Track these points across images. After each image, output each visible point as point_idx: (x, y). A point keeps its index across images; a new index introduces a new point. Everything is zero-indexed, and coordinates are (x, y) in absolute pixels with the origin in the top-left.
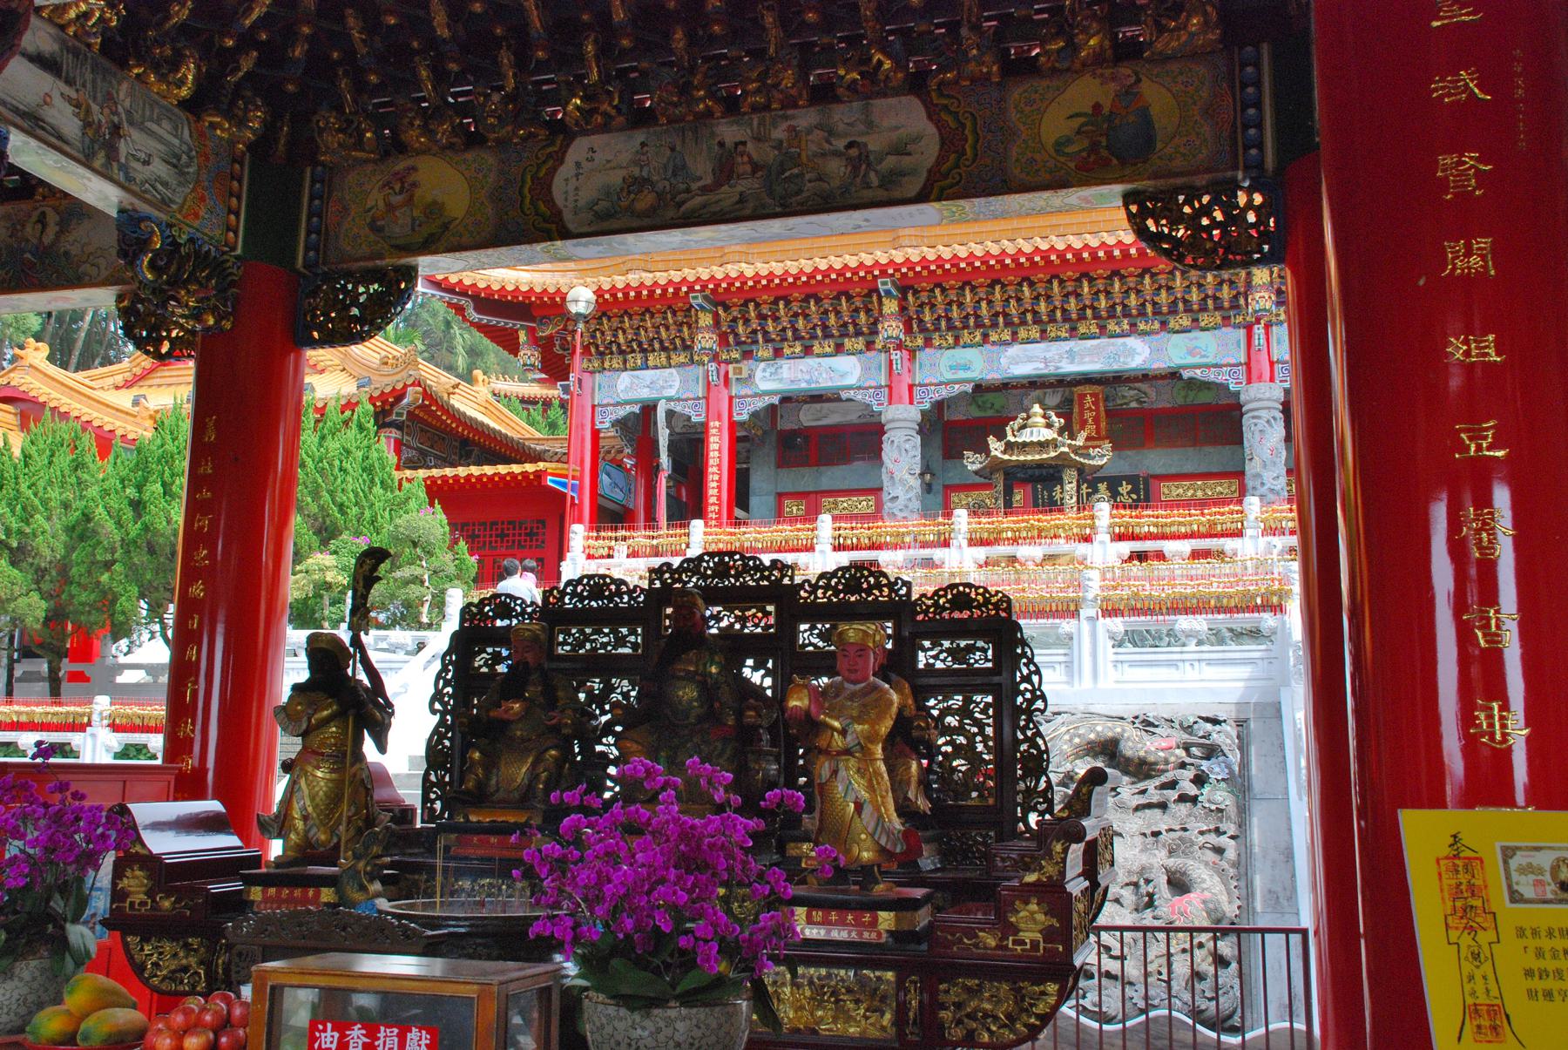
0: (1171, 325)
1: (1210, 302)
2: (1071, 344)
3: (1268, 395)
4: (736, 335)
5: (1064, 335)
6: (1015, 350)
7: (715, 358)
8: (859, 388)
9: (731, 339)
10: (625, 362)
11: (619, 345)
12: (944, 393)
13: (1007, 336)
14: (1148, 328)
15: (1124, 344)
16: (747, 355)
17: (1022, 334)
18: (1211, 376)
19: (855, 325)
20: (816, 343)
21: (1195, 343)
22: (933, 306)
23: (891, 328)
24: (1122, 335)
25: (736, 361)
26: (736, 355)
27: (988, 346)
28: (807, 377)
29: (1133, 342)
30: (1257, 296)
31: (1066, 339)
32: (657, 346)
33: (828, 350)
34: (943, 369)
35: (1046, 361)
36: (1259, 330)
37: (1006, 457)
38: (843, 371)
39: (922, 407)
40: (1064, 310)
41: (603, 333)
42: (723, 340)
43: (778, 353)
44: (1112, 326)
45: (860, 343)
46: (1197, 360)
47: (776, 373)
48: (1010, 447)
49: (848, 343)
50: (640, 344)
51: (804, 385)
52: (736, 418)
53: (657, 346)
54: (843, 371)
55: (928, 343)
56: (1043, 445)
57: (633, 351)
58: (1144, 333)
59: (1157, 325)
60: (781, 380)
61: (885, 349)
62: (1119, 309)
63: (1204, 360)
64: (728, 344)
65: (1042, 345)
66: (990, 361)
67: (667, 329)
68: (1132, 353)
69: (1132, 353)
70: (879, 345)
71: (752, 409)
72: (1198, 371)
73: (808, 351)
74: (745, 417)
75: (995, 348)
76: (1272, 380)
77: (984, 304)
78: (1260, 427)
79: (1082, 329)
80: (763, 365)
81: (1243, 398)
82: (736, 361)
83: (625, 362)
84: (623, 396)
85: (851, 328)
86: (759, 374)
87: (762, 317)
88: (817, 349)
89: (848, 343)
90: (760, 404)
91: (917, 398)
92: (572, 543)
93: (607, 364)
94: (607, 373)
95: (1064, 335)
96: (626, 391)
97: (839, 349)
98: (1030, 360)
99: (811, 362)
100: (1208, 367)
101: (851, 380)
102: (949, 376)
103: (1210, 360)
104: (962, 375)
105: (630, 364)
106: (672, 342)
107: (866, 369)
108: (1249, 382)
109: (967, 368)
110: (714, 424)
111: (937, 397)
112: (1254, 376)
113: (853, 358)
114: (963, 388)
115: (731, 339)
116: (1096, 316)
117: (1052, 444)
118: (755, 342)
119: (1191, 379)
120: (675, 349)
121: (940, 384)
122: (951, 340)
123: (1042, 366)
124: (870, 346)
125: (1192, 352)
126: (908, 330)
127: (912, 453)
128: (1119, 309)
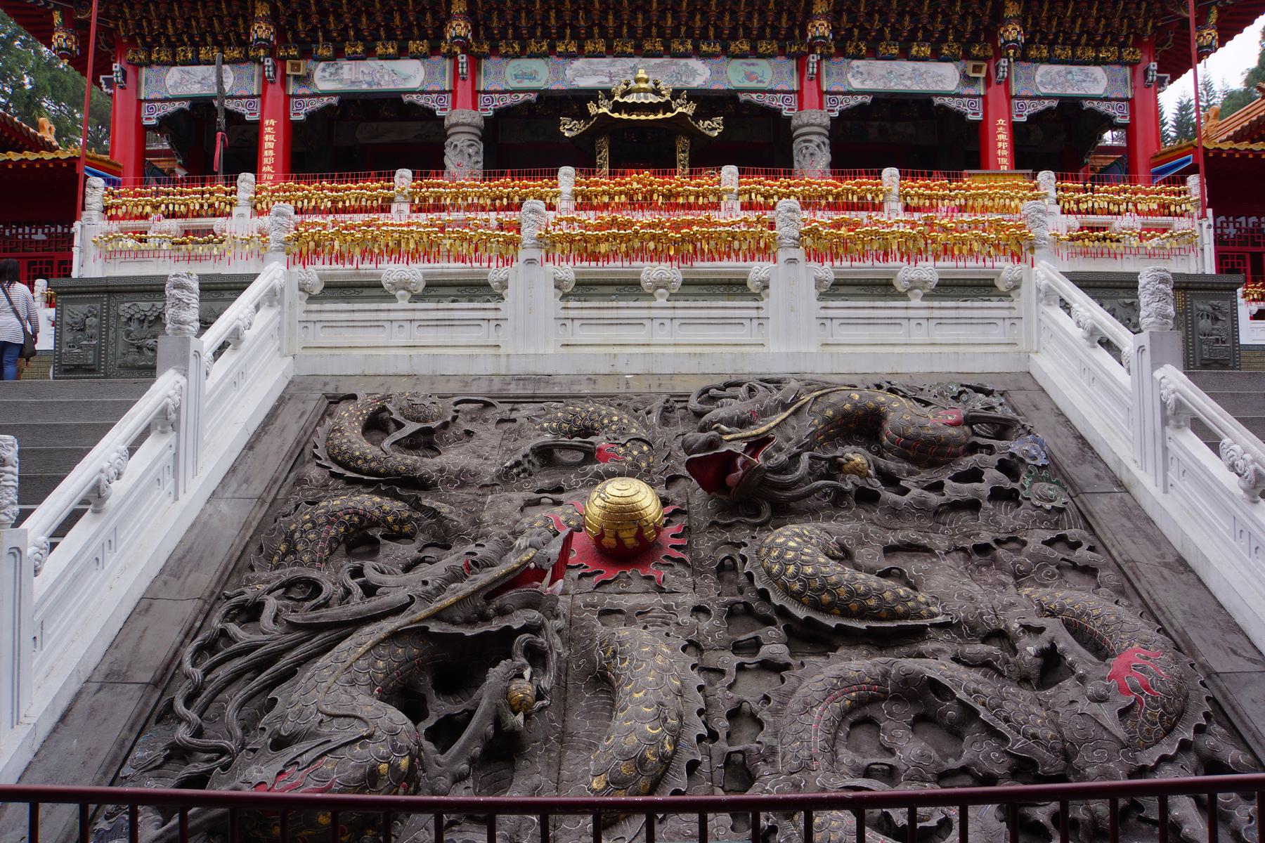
0: (732, 48)
1: (768, 30)
2: (636, 60)
3: (818, 121)
4: (296, 33)
5: (630, 50)
6: (580, 63)
7: (272, 53)
8: (422, 92)
9: (289, 36)
10: (174, 55)
11: (168, 38)
12: (509, 100)
13: (573, 48)
14: (710, 50)
15: (686, 65)
16: (307, 54)
17: (589, 47)
18: (767, 100)
19: (420, 28)
20: (379, 43)
21: (752, 69)
22: (501, 13)
23: (459, 28)
24: (686, 55)
25: (293, 57)
26: (293, 52)
27: (554, 59)
28: (369, 79)
29: (694, 63)
30: (817, 23)
31: (630, 56)
32: (209, 39)
33: (391, 50)
34: (508, 77)
35: (610, 75)
36: (813, 59)
37: (616, 115)
38: (407, 75)
39: (486, 114)
40: (630, 27)
41: (150, 22)
42: (280, 34)
43: (339, 54)
44: (676, 45)
45: (423, 46)
46: (754, 85)
47: (336, 73)
48: (617, 107)
49: (412, 46)
50: (191, 38)
51: (365, 87)
52: (293, 118)
53: (209, 39)
54: (407, 75)
55: (494, 51)
56: (652, 108)
57: (184, 44)
58: (705, 56)
59: (718, 48)
60: (341, 81)
61: (452, 55)
62: (683, 29)
63: (760, 85)
64: (287, 41)
65: (607, 60)
66: (555, 72)
67: (221, 22)
68: (693, 73)
69: (693, 73)
70: (444, 48)
71: (309, 108)
72: (754, 96)
73: (369, 53)
74: (302, 117)
75: (561, 60)
76: (821, 107)
77: (553, 14)
78: (810, 150)
79: (648, 46)
80: (322, 65)
81: (794, 122)
82: (293, 57)
83: (174, 55)
84: (172, 92)
85: (415, 31)
86: (318, 74)
87: (323, 13)
88: (380, 50)
89: (412, 46)
90: (318, 104)
91: (481, 105)
92: (88, 200)
93: (154, 57)
94: (156, 68)
95: (630, 50)
96: (175, 86)
97: (402, 53)
98: (595, 73)
99: (373, 64)
100: (764, 92)
101: (415, 84)
102: (514, 84)
103: (766, 85)
104: (527, 84)
105: (180, 57)
106: (227, 38)
107: (430, 74)
108: (801, 108)
109: (532, 77)
110: (269, 123)
111: (501, 104)
112: (806, 103)
113: (416, 64)
114: (528, 97)
115: (289, 36)
116: (661, 34)
117: (666, 107)
118: (317, 42)
119: (748, 103)
120: (229, 45)
121: (506, 92)
122: (517, 49)
123: (607, 79)
124: (434, 50)
125: (749, 77)
126: (475, 36)
127: (474, 159)
128: (683, 29)
